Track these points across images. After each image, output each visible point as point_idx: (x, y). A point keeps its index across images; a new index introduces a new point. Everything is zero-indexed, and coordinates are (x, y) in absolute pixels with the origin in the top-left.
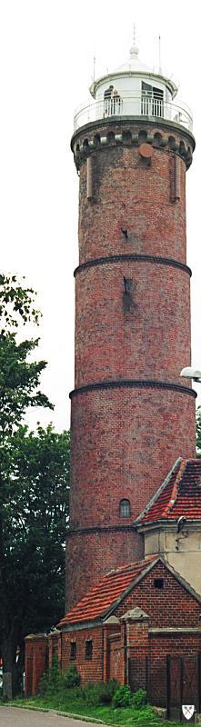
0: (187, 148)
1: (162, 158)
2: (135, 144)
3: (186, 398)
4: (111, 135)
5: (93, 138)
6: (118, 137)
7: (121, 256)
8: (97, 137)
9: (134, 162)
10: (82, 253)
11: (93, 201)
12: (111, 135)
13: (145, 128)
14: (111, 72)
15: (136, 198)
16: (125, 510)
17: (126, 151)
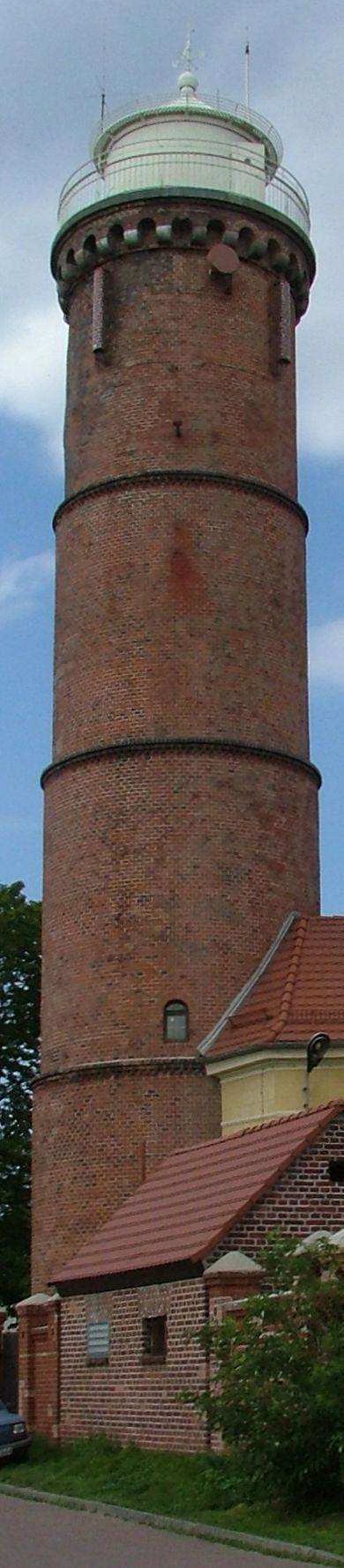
0: (301, 272)
1: (254, 282)
2: (199, 247)
4: (147, 226)
5: (106, 231)
6: (163, 229)
7: (168, 474)
8: (117, 231)
9: (197, 283)
11: (105, 357)
12: (147, 226)
15: (198, 357)
16: (175, 1025)
17: (178, 260)
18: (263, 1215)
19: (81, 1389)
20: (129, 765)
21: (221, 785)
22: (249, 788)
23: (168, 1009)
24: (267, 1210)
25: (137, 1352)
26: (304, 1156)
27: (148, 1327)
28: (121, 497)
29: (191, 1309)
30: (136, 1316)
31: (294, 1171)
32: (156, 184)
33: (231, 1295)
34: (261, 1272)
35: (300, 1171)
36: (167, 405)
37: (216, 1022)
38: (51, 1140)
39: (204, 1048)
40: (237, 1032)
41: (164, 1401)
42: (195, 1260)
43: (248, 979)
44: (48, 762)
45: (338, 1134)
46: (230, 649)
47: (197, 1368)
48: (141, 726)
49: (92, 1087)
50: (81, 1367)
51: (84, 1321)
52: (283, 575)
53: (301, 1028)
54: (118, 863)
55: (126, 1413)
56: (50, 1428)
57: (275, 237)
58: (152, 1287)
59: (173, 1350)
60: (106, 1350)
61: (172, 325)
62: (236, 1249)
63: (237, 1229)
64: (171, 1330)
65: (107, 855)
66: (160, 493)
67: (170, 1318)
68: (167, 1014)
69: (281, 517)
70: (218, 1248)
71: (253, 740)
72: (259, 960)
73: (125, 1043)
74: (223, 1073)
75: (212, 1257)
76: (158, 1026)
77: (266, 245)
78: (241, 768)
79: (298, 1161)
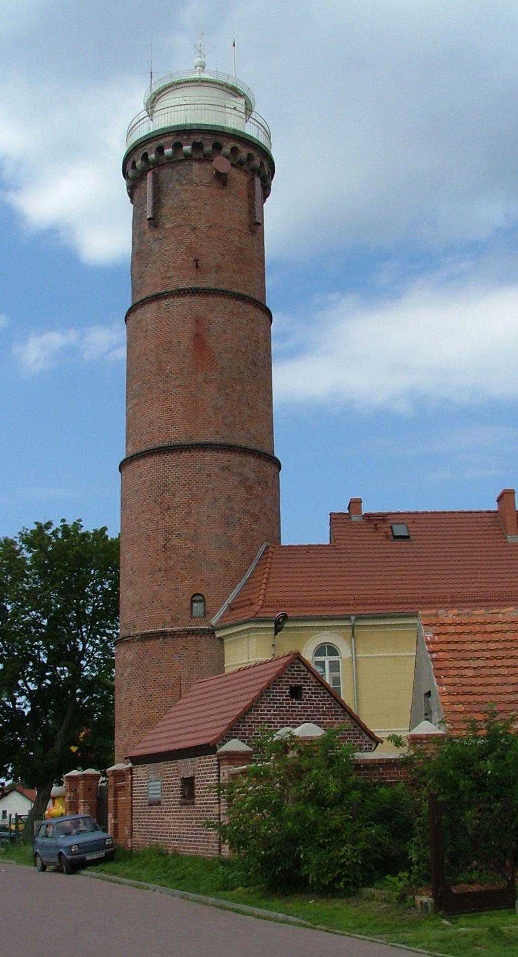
0: (267, 172)
1: (239, 178)
2: (208, 159)
3: (271, 469)
4: (177, 147)
6: (187, 148)
8: (160, 150)
9: (207, 178)
10: (135, 291)
11: (154, 222)
12: (177, 147)
13: (220, 139)
14: (176, 79)
15: (208, 221)
16: (198, 608)
17: (196, 166)
18: (251, 718)
19: (145, 818)
20: (170, 458)
21: (223, 469)
23: (194, 599)
24: (254, 715)
25: (177, 798)
26: (275, 683)
27: (184, 783)
28: (164, 303)
29: (210, 773)
30: (177, 776)
31: (270, 692)
32: (182, 122)
33: (233, 765)
34: (250, 752)
35: (273, 692)
36: (190, 250)
37: (221, 607)
38: (126, 674)
39: (214, 621)
40: (233, 612)
41: (193, 826)
42: (211, 745)
43: (240, 581)
44: (123, 457)
45: (295, 671)
46: (228, 390)
47: (213, 807)
48: (177, 435)
49: (150, 644)
50: (145, 806)
51: (146, 779)
52: (258, 348)
53: (271, 609)
54: (164, 515)
55: (171, 833)
56: (127, 842)
57: (251, 152)
58: (186, 760)
59: (199, 796)
60: (159, 796)
61: (193, 203)
62: (236, 738)
63: (236, 726)
64: (197, 785)
65: (158, 510)
66: (186, 300)
67: (197, 778)
68: (193, 602)
69: (259, 315)
70: (226, 737)
71: (241, 443)
72: (246, 570)
73: (168, 619)
74: (223, 636)
75: (221, 742)
76: (188, 609)
77: (246, 156)
78: (233, 459)
79: (272, 686)
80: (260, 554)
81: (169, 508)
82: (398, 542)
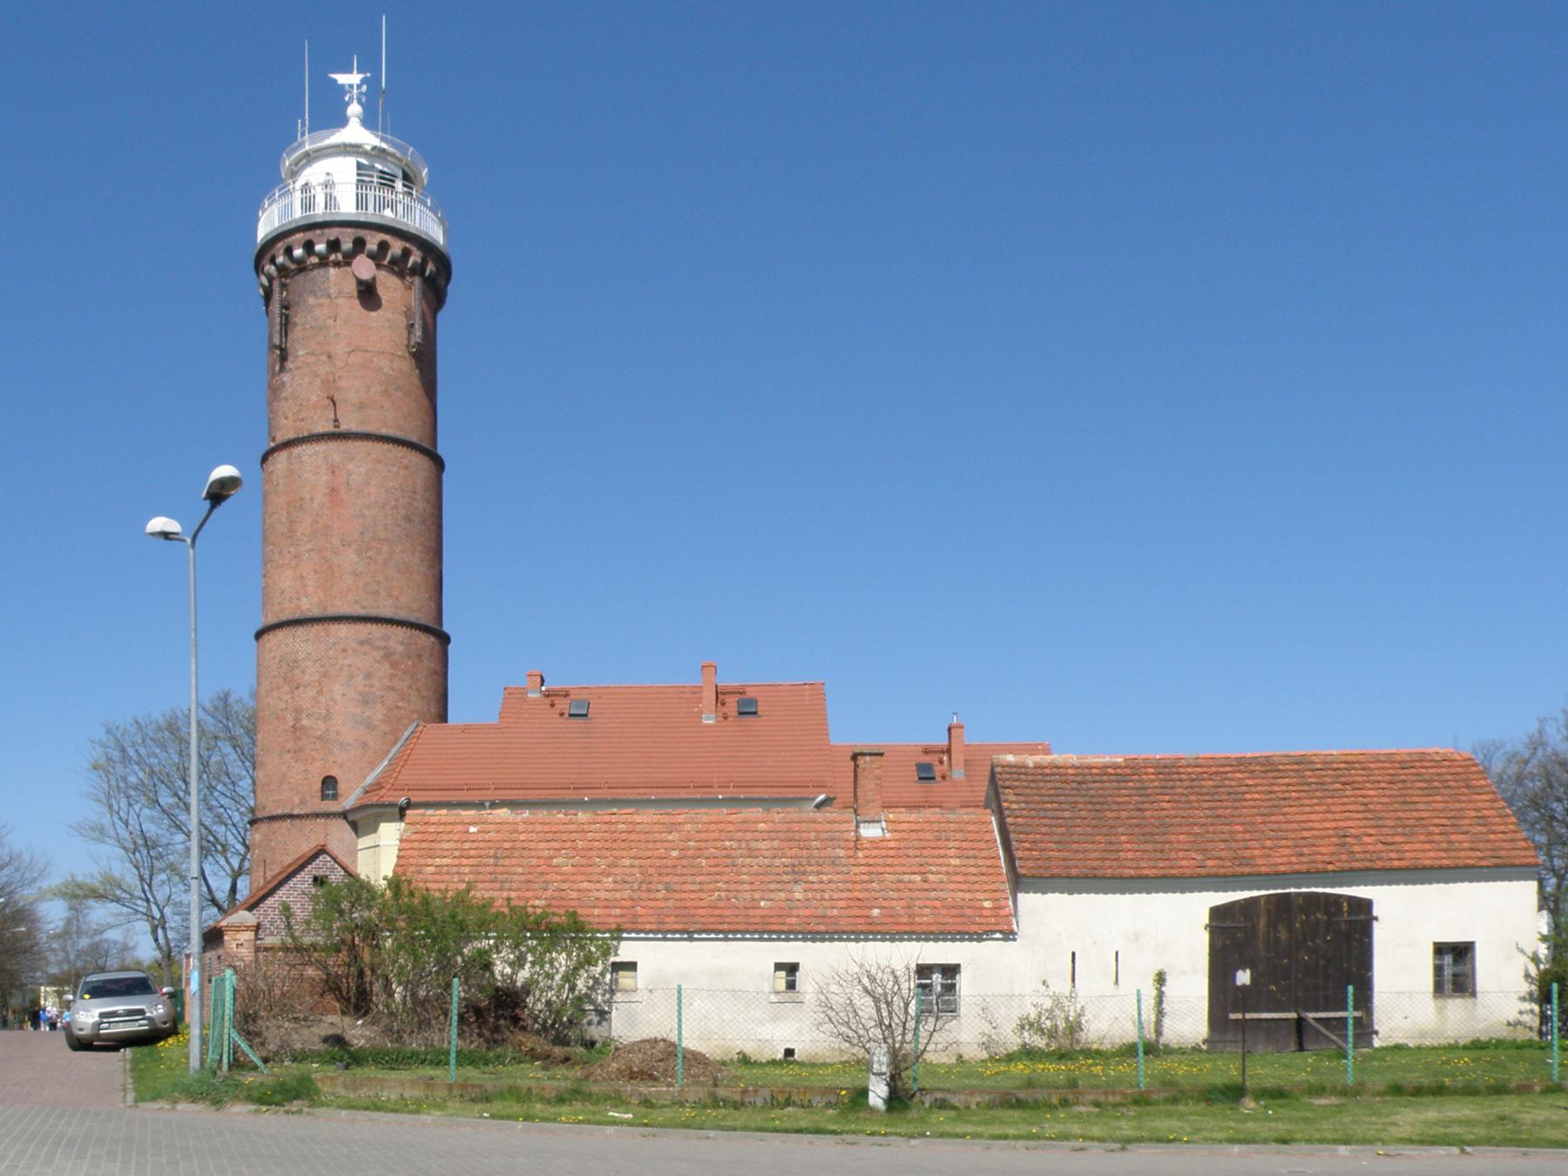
4: (309, 246)
5: (282, 251)
9: (352, 287)
21: (362, 643)
22: (382, 644)
65: (286, 688)
66: (320, 447)
71: (387, 612)
72: (389, 751)
73: (297, 801)
78: (376, 631)
80: (407, 734)
81: (297, 688)
82: (573, 720)
